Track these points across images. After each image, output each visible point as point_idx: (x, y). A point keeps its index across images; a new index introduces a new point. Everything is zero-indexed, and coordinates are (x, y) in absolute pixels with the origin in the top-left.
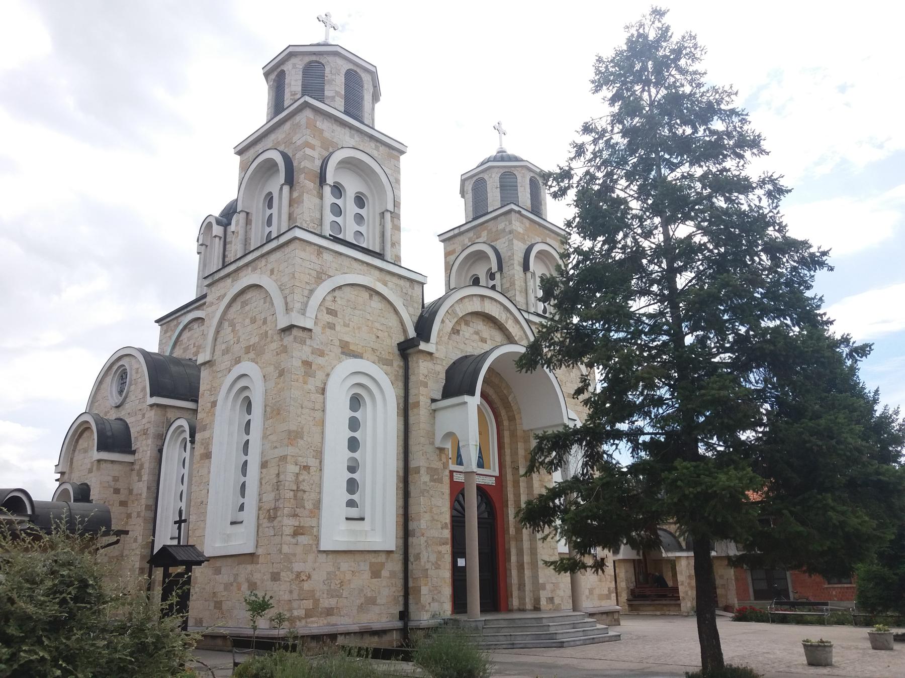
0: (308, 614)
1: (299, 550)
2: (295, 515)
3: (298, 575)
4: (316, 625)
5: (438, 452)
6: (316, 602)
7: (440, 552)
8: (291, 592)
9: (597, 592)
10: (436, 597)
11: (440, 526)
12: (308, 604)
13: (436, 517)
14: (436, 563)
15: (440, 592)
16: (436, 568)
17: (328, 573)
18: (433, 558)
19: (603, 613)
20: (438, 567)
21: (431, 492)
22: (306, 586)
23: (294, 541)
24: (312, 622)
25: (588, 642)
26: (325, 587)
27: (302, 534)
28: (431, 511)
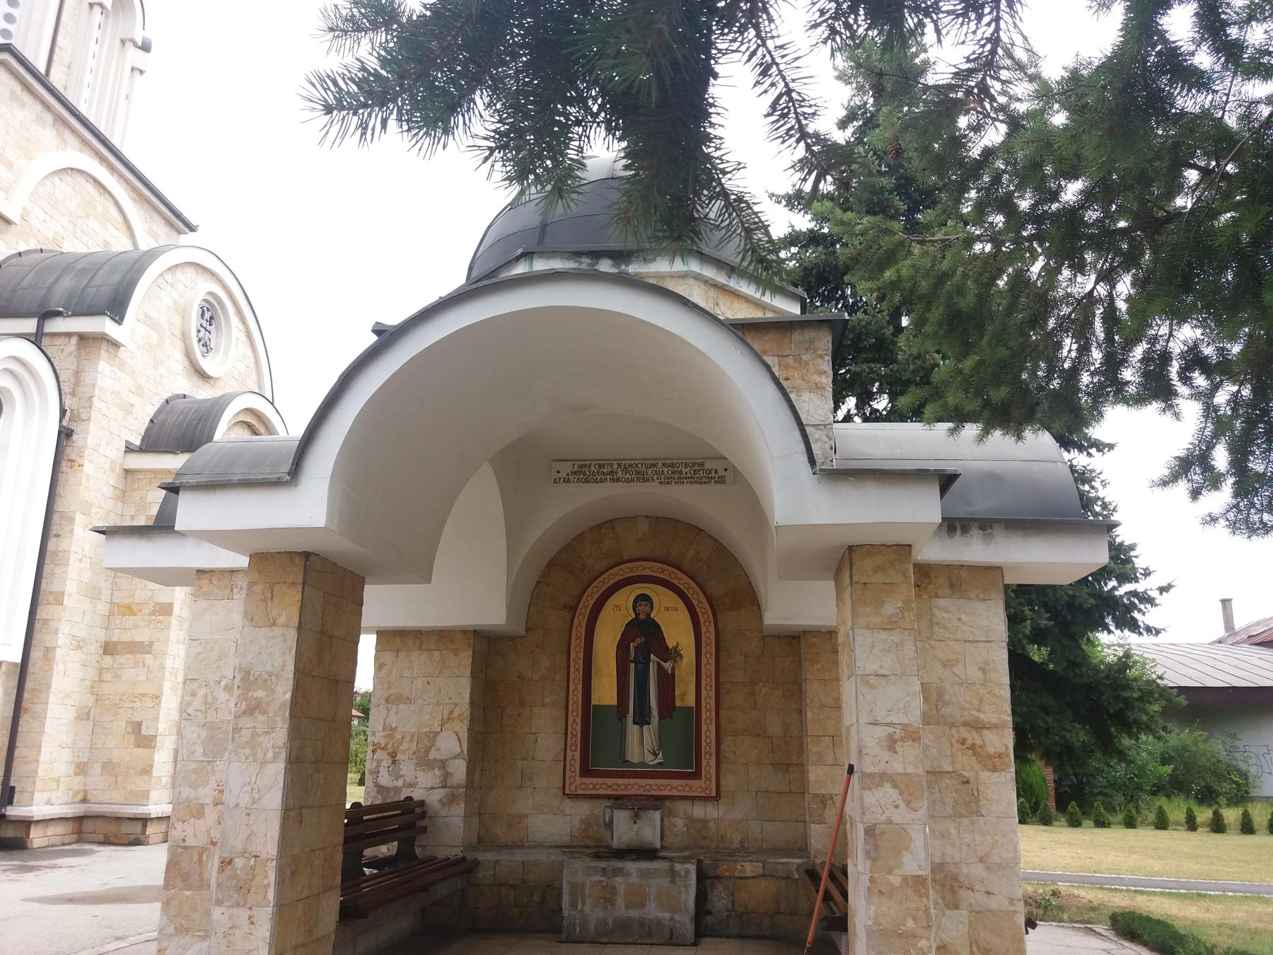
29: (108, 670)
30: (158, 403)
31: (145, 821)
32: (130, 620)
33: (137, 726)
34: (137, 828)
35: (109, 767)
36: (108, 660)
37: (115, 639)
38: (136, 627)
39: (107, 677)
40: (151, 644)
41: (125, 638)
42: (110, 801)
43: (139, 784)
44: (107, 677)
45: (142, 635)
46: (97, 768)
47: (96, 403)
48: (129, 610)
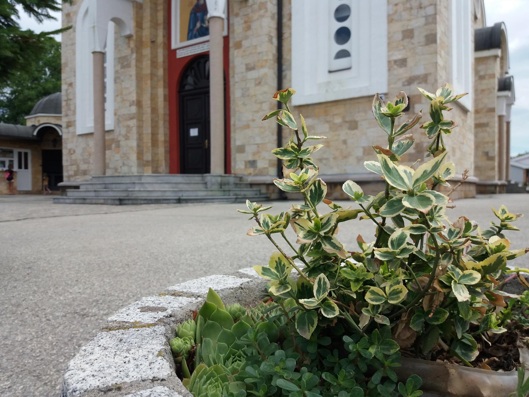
0: (76, 174)
2: (67, 115)
3: (70, 150)
4: (79, 180)
5: (127, 41)
6: (78, 166)
7: (128, 126)
10: (125, 162)
11: (128, 104)
12: (74, 168)
14: (126, 135)
15: (128, 158)
16: (126, 139)
17: (83, 149)
18: (123, 131)
20: (127, 138)
21: (122, 78)
22: (74, 157)
24: (78, 179)
27: (70, 126)
28: (122, 94)
34: (493, 189)
43: (491, 173)
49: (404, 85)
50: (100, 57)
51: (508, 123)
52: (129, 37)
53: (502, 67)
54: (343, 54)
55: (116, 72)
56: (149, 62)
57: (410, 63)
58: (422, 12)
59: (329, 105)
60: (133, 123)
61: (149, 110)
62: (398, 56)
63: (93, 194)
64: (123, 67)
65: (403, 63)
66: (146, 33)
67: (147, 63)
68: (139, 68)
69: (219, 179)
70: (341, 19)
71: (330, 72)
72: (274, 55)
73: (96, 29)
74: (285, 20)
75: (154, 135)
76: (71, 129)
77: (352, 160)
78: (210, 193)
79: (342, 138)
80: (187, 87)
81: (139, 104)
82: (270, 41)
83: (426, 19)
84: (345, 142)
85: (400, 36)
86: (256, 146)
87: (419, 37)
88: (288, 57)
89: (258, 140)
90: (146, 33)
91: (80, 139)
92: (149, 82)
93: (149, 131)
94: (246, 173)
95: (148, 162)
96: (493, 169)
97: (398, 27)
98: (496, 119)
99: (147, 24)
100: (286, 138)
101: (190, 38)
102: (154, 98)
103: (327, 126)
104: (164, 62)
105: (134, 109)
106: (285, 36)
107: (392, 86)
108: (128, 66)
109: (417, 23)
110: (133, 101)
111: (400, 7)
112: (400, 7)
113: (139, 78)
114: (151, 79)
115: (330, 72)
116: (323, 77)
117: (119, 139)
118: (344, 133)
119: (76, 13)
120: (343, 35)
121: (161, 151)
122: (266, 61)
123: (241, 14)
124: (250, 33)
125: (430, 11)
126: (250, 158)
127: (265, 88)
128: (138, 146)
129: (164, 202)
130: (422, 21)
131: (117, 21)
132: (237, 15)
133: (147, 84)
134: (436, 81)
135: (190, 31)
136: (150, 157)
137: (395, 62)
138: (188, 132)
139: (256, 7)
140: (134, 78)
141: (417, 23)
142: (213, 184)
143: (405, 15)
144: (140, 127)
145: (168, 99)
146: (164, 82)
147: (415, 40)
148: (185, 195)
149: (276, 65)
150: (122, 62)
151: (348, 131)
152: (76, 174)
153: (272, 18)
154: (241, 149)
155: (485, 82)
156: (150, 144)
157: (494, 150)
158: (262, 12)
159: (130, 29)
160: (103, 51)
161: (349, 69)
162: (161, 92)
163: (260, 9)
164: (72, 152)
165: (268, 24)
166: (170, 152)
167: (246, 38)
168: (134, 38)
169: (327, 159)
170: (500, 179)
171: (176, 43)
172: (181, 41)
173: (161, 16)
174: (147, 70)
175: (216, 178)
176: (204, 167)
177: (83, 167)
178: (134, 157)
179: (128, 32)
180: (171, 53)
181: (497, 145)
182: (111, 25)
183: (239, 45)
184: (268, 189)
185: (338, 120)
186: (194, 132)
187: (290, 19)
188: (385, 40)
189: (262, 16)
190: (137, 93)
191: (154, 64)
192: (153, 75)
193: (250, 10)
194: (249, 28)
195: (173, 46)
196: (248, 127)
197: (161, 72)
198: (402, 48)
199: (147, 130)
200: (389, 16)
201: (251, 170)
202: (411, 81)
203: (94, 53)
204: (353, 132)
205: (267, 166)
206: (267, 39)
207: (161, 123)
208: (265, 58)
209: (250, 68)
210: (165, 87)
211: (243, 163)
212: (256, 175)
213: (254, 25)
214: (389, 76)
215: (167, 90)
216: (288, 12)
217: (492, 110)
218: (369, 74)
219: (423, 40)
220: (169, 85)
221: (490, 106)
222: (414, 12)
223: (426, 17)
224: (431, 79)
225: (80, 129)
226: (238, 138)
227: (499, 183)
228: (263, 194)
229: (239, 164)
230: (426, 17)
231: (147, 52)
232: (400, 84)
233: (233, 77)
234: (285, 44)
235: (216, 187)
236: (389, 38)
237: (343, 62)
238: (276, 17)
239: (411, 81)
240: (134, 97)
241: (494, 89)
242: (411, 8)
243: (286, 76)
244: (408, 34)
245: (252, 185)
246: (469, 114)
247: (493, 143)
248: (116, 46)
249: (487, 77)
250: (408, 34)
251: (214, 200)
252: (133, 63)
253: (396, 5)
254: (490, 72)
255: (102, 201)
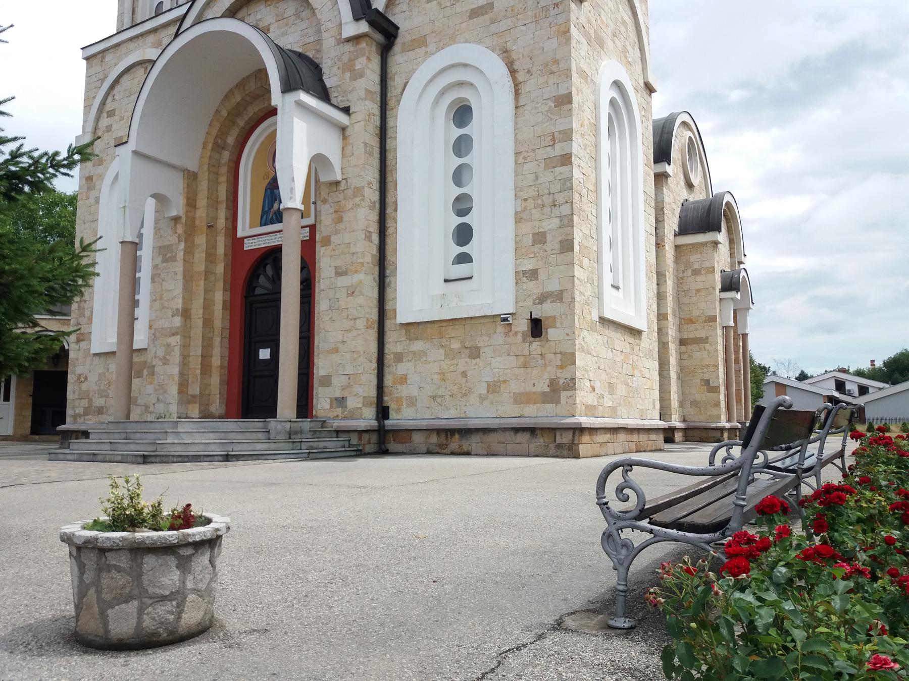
0: (86, 413)
1: (81, 354)
5: (172, 223)
6: (90, 401)
7: (169, 345)
8: (74, 393)
9: (515, 387)
10: (161, 397)
11: (170, 314)
12: (85, 403)
13: (166, 304)
14: (164, 358)
15: (165, 392)
16: (164, 364)
18: (161, 352)
19: (517, 430)
20: (165, 362)
21: (163, 275)
22: (84, 387)
23: (77, 347)
24: (89, 420)
25: (85, 457)
26: (96, 388)
27: (83, 340)
28: (161, 298)
29: (684, 353)
30: (680, 205)
31: (722, 430)
32: (692, 327)
33: (707, 382)
34: (718, 434)
35: (695, 403)
36: (683, 348)
37: (685, 337)
38: (696, 330)
39: (685, 357)
40: (707, 338)
41: (691, 336)
42: (699, 420)
43: (714, 411)
44: (685, 357)
45: (701, 334)
46: (688, 404)
47: (666, 212)
48: (691, 321)
49: (534, 304)
50: (131, 248)
51: (745, 336)
52: (176, 219)
53: (732, 255)
54: (463, 258)
55: (155, 267)
56: (204, 255)
57: (542, 276)
58: (556, 211)
59: (444, 324)
60: (176, 340)
61: (200, 323)
62: (527, 266)
63: (108, 447)
64: (165, 260)
65: (533, 274)
66: (201, 213)
67: (200, 256)
68: (188, 263)
69: (288, 425)
70: (462, 213)
71: (446, 281)
72: (373, 255)
73: (127, 210)
74: (389, 210)
75: (206, 358)
76: (83, 345)
77: (473, 399)
78: (273, 446)
79: (461, 368)
80: (258, 291)
81: (186, 313)
82: (369, 238)
83: (561, 221)
84: (464, 374)
85: (529, 240)
86: (347, 377)
87: (553, 243)
88: (393, 259)
89: (349, 370)
90: (201, 213)
91: (96, 360)
92: (202, 283)
93: (199, 352)
94: (331, 415)
95: (193, 396)
96: (717, 404)
97: (527, 228)
98: (719, 332)
99: (202, 202)
100: (389, 366)
101: (262, 224)
102: (208, 306)
103: (442, 351)
104: (225, 255)
105: (177, 321)
106: (390, 231)
107: (521, 304)
108: (173, 259)
109: (550, 225)
110: (177, 310)
111: (530, 204)
112: (530, 204)
113: (188, 277)
114: (205, 280)
115: (446, 281)
116: (440, 288)
117: (154, 363)
118: (463, 363)
119: (101, 177)
120: (463, 234)
121: (215, 381)
122: (362, 264)
123: (330, 200)
124: (341, 226)
125: (565, 210)
126: (338, 394)
127: (361, 300)
128: (181, 374)
129: (206, 459)
130: (557, 222)
131: (160, 198)
132: (325, 201)
133: (200, 286)
134: (573, 299)
135: (264, 213)
136: (198, 390)
137: (524, 272)
138: (257, 354)
139: (350, 192)
140: (180, 276)
141: (550, 225)
142: (278, 433)
143: (536, 213)
144: (185, 347)
145: (230, 306)
146: (225, 282)
147: (548, 247)
148: (237, 450)
149: (377, 268)
150: (164, 253)
151: (469, 360)
152: (86, 413)
153: (372, 208)
154: (327, 381)
155: (699, 278)
156: (198, 372)
157: (718, 378)
158: (358, 199)
159: (177, 208)
160: (137, 241)
161: (471, 278)
162: (219, 297)
163: (355, 196)
164: (82, 379)
165: (367, 217)
166: (228, 382)
167: (337, 232)
168: (183, 220)
169: (442, 396)
170: (729, 420)
171: (244, 229)
172: (252, 226)
173: (223, 191)
174: (200, 267)
175: (283, 424)
176: (268, 409)
177: (98, 402)
178: (173, 390)
179: (174, 213)
180: (236, 243)
181: (721, 369)
182: (151, 204)
183: (327, 241)
184: (360, 439)
185: (456, 345)
186: (264, 354)
187: (396, 210)
188: (511, 246)
189: (358, 206)
190: (184, 298)
191: (210, 257)
192: (207, 273)
193: (341, 196)
194: (340, 220)
195: (240, 234)
196: (336, 350)
197: (220, 269)
198: (532, 256)
199: (196, 351)
200: (516, 213)
201: (338, 411)
202: (542, 299)
203: (122, 243)
204: (474, 361)
205: (360, 405)
206: (363, 236)
207: (217, 341)
208: (361, 261)
209: (340, 273)
210: (225, 290)
211: (328, 401)
212: (345, 418)
213: (347, 217)
214: (517, 291)
215: (229, 293)
216: (394, 199)
217: (713, 319)
218: (493, 289)
219: (557, 246)
220: (231, 286)
221: (710, 313)
222: (547, 210)
223: (561, 217)
224: (566, 297)
225: (96, 347)
226: (322, 366)
227: (727, 425)
228: (354, 445)
229: (322, 402)
230: (561, 217)
231: (201, 240)
232: (529, 302)
233: (319, 282)
234: (389, 241)
235: (283, 437)
236: (516, 243)
237: (462, 270)
238: (377, 205)
239: (542, 299)
240: (179, 304)
241: (714, 288)
242: (543, 206)
243: (390, 282)
244: (540, 238)
245: (338, 432)
246: (644, 335)
247: (716, 366)
248: (157, 230)
249: (703, 272)
250: (540, 238)
251: (277, 457)
252: (180, 255)
253: (526, 200)
254: (707, 264)
255: (119, 458)
